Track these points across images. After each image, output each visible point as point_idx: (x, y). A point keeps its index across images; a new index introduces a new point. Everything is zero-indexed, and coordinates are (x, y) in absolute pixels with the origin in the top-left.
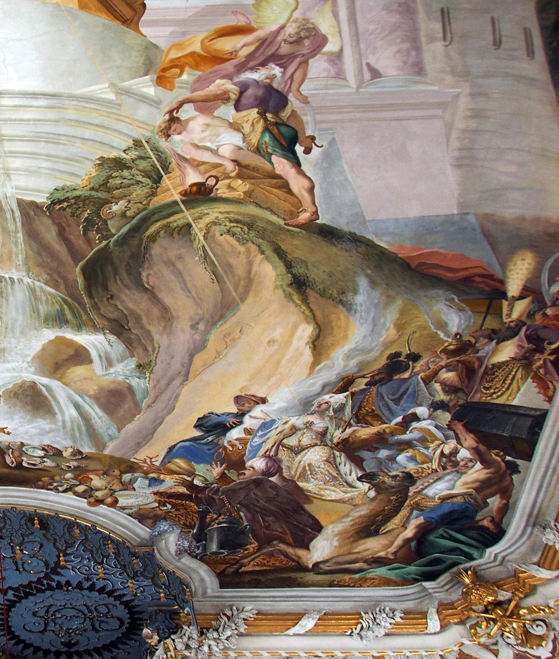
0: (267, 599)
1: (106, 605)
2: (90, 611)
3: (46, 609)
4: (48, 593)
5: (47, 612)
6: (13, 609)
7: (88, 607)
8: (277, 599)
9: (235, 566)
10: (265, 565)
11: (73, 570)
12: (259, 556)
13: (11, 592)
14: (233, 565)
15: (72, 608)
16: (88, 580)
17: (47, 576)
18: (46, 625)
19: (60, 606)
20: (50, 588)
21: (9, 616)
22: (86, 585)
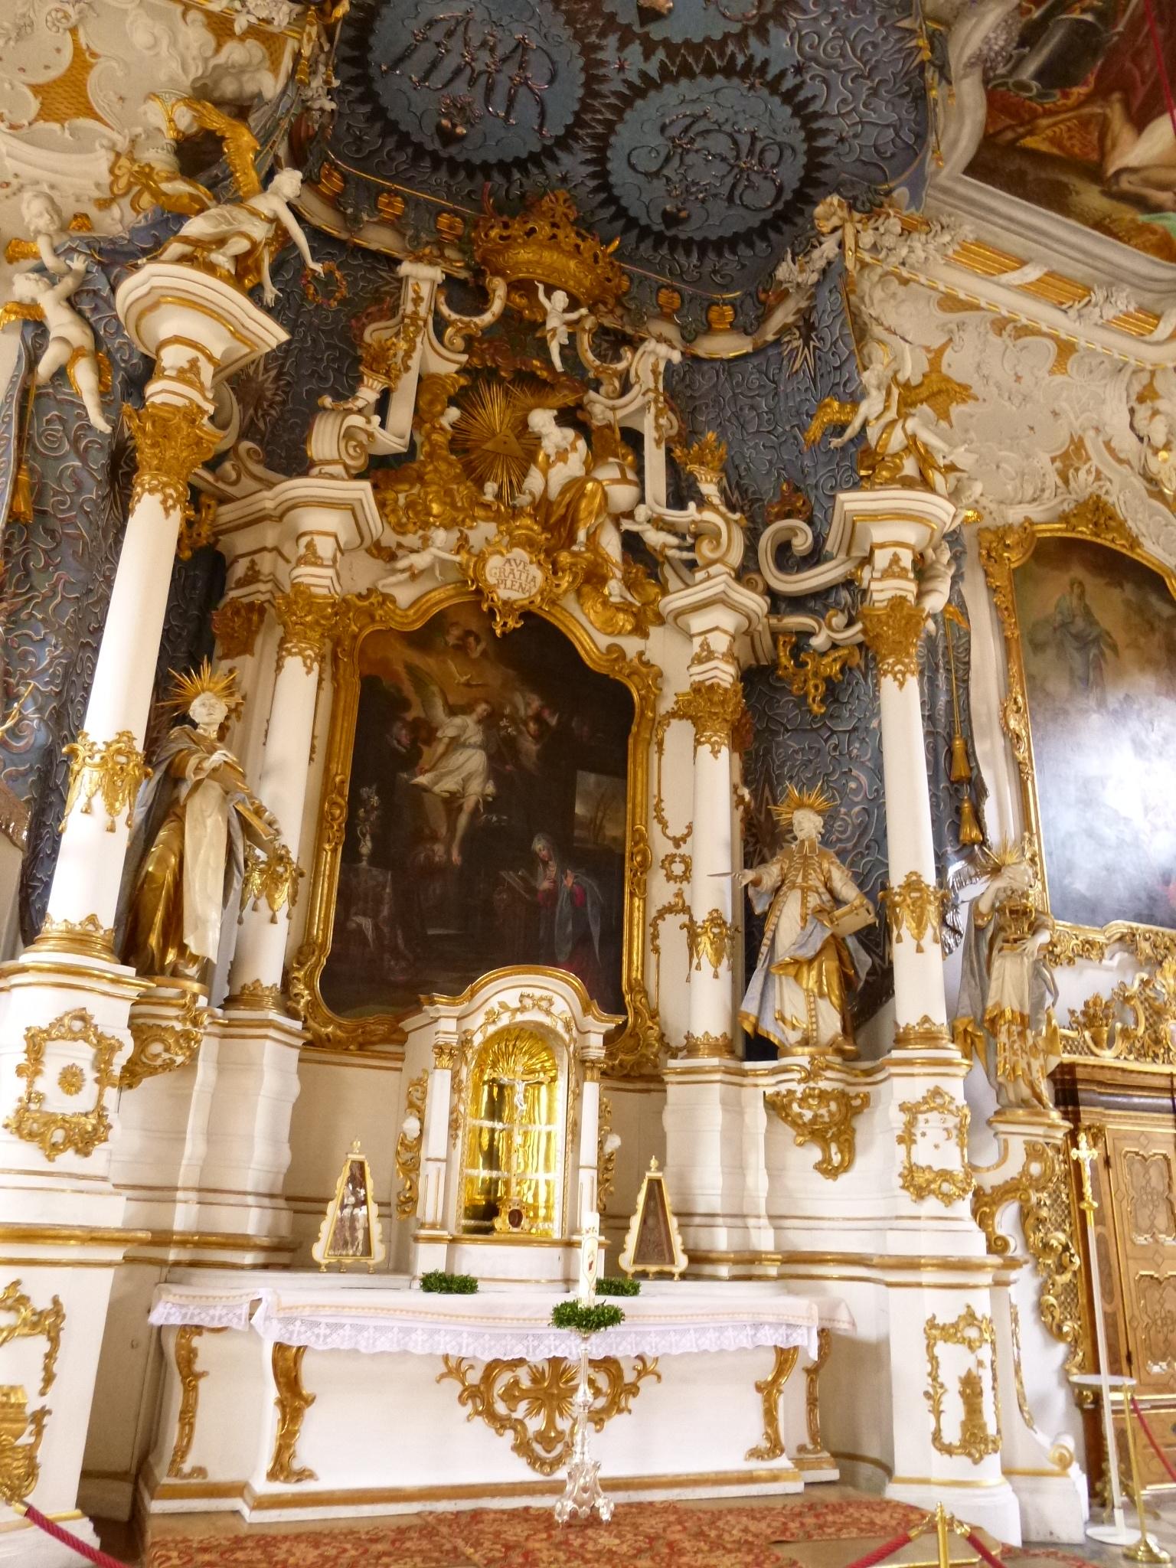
0: (1001, 222)
1: (781, 146)
2: (751, 153)
3: (688, 121)
4: (719, 80)
5: (686, 130)
6: (639, 103)
7: (754, 138)
8: (1013, 227)
9: (1021, 130)
10: (1061, 147)
11: (792, 38)
12: (1069, 119)
13: (661, 54)
14: (1022, 125)
15: (731, 135)
16: (799, 70)
17: (741, 38)
18: (668, 159)
19: (716, 122)
20: (729, 71)
21: (621, 119)
22: (789, 83)
